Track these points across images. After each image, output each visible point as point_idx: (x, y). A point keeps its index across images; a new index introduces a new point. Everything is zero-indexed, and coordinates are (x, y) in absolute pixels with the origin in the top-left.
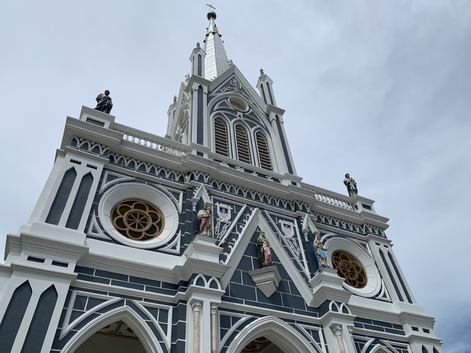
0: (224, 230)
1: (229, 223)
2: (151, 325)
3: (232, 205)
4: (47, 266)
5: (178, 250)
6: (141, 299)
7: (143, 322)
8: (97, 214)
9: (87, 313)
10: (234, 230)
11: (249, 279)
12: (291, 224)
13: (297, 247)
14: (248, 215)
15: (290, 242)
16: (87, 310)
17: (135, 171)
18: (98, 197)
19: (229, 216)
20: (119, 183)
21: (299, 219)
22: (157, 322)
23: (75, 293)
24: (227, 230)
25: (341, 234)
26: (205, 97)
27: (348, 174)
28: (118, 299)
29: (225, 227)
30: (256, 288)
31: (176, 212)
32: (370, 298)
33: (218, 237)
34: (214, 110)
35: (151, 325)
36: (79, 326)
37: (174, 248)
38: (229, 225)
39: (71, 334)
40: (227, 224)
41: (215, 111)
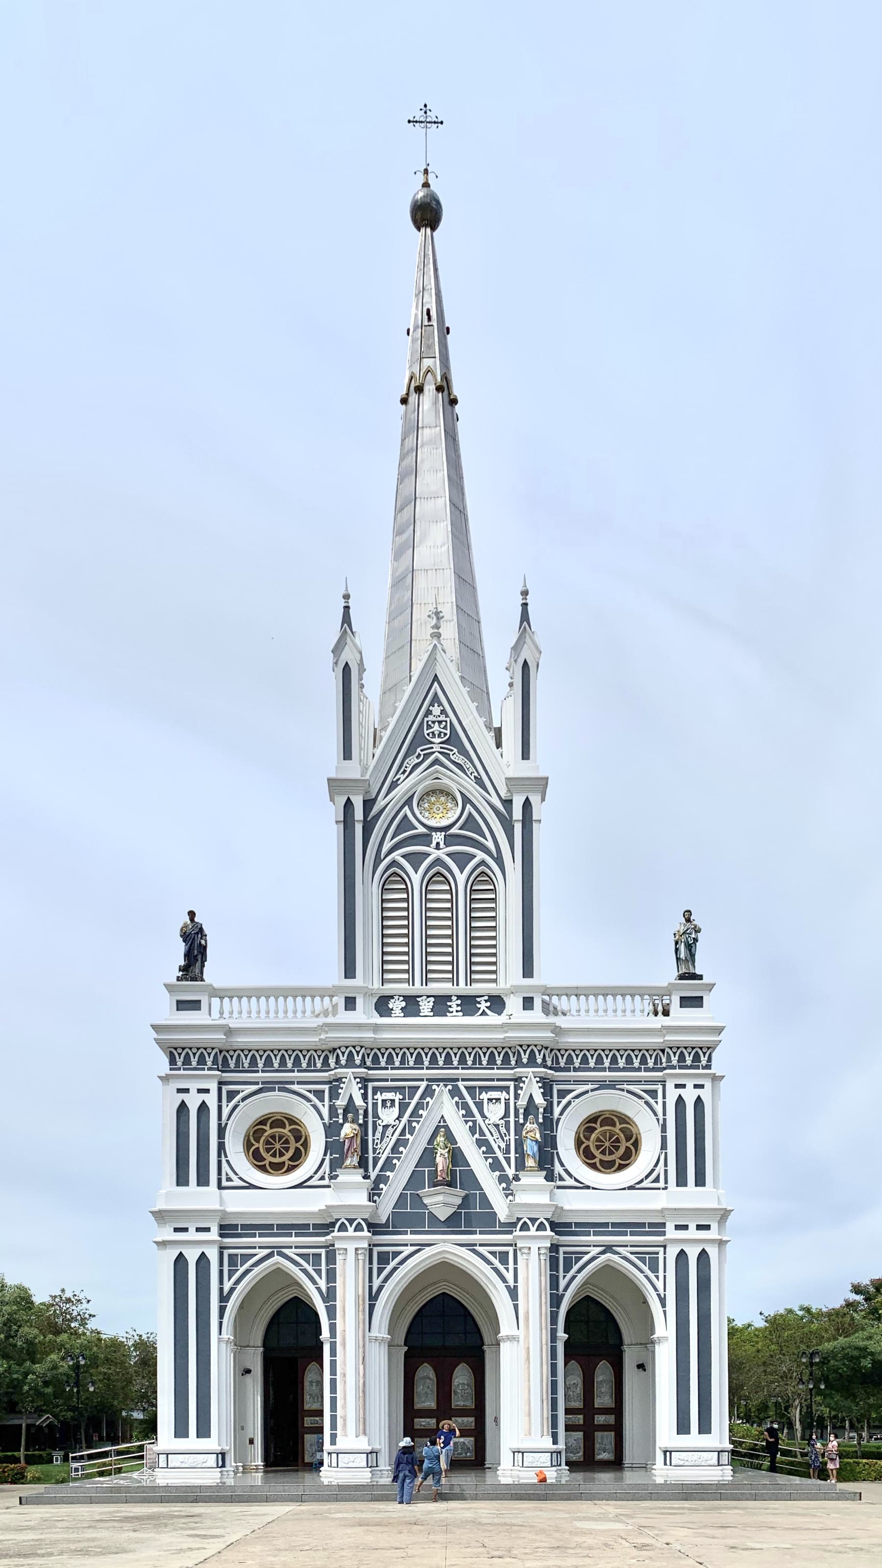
0: (388, 1137)
1: (395, 1124)
6: (291, 1247)
8: (226, 1156)
9: (242, 1270)
10: (403, 1133)
11: (418, 1200)
12: (503, 1095)
13: (505, 1134)
14: (428, 1099)
15: (493, 1129)
16: (241, 1266)
17: (257, 1071)
19: (396, 1111)
20: (243, 1099)
22: (310, 1269)
23: (226, 1253)
24: (392, 1136)
25: (609, 1081)
27: (689, 911)
28: (266, 1252)
29: (391, 1130)
30: (427, 1211)
31: (321, 1122)
32: (624, 1189)
33: (378, 1152)
34: (382, 859)
36: (237, 1282)
37: (322, 1178)
38: (395, 1128)
39: (232, 1290)
40: (393, 1127)
41: (384, 858)
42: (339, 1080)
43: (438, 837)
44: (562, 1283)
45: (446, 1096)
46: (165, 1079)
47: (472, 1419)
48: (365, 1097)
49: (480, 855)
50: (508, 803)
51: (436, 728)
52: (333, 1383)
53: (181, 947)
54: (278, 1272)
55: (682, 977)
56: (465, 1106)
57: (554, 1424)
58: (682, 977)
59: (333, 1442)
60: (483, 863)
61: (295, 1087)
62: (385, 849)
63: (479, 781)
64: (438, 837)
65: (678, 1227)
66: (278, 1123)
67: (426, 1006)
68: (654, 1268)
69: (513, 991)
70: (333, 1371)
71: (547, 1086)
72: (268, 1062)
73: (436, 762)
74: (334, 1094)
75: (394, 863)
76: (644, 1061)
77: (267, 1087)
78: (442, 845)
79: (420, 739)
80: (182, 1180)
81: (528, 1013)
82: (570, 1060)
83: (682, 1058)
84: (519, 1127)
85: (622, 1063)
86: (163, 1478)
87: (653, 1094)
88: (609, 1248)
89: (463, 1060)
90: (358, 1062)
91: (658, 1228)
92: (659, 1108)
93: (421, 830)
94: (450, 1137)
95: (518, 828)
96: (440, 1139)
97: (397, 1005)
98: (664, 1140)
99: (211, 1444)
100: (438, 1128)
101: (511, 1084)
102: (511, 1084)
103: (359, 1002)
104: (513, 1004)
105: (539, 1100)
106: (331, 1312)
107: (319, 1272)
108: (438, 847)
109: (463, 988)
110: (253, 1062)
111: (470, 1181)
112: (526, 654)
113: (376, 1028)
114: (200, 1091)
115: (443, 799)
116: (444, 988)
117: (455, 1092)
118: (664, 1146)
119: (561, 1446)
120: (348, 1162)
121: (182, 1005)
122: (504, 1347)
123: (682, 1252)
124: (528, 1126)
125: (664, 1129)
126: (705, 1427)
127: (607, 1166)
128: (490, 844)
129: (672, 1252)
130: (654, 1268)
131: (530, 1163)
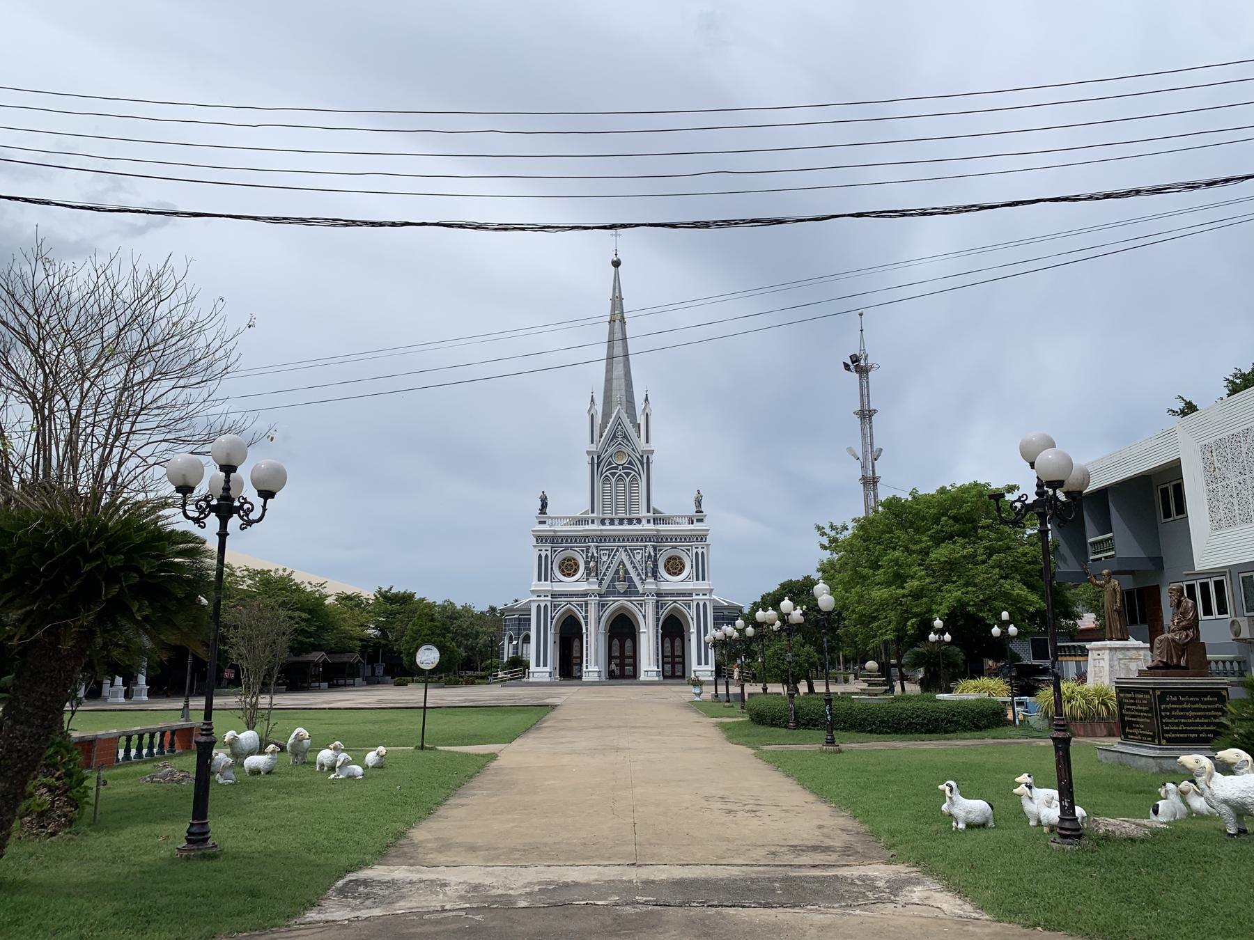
2: (578, 610)
3: (608, 550)
4: (542, 598)
5: (585, 580)
7: (575, 609)
11: (614, 586)
18: (552, 564)
20: (559, 553)
21: (646, 546)
22: (579, 609)
26: (596, 466)
35: (578, 610)
39: (555, 616)
42: (589, 547)
43: (620, 467)
44: (660, 614)
45: (623, 552)
46: (535, 546)
47: (632, 660)
48: (597, 552)
49: (634, 473)
50: (642, 456)
51: (620, 433)
52: (587, 647)
53: (540, 503)
54: (569, 610)
55: (697, 512)
56: (629, 555)
57: (658, 662)
58: (697, 512)
59: (587, 668)
60: (634, 475)
61: (575, 549)
62: (604, 470)
63: (633, 449)
64: (620, 467)
65: (696, 595)
66: (569, 560)
67: (616, 522)
68: (689, 608)
69: (644, 517)
70: (587, 644)
71: (655, 548)
72: (567, 540)
73: (620, 444)
74: (587, 551)
75: (606, 476)
76: (685, 539)
77: (567, 548)
79: (615, 437)
80: (539, 580)
81: (649, 525)
82: (662, 539)
83: (697, 539)
84: (646, 562)
85: (678, 540)
86: (531, 680)
87: (688, 550)
88: (675, 602)
89: (628, 540)
90: (595, 540)
91: (690, 595)
92: (690, 555)
93: (616, 465)
94: (624, 565)
95: (645, 465)
96: (621, 566)
97: (607, 522)
98: (692, 565)
99: (548, 669)
100: (620, 562)
101: (644, 548)
102: (644, 548)
103: (595, 522)
104: (644, 521)
105: (652, 554)
106: (586, 624)
107: (582, 610)
109: (628, 516)
110: (562, 540)
111: (631, 580)
112: (647, 410)
113: (601, 530)
114: (546, 550)
116: (622, 515)
117: (626, 550)
118: (692, 567)
119: (660, 669)
120: (592, 575)
121: (541, 523)
122: (642, 635)
123: (698, 603)
124: (649, 562)
125: (692, 562)
126: (707, 663)
127: (675, 574)
128: (637, 470)
129: (695, 603)
130: (690, 608)
131: (649, 575)
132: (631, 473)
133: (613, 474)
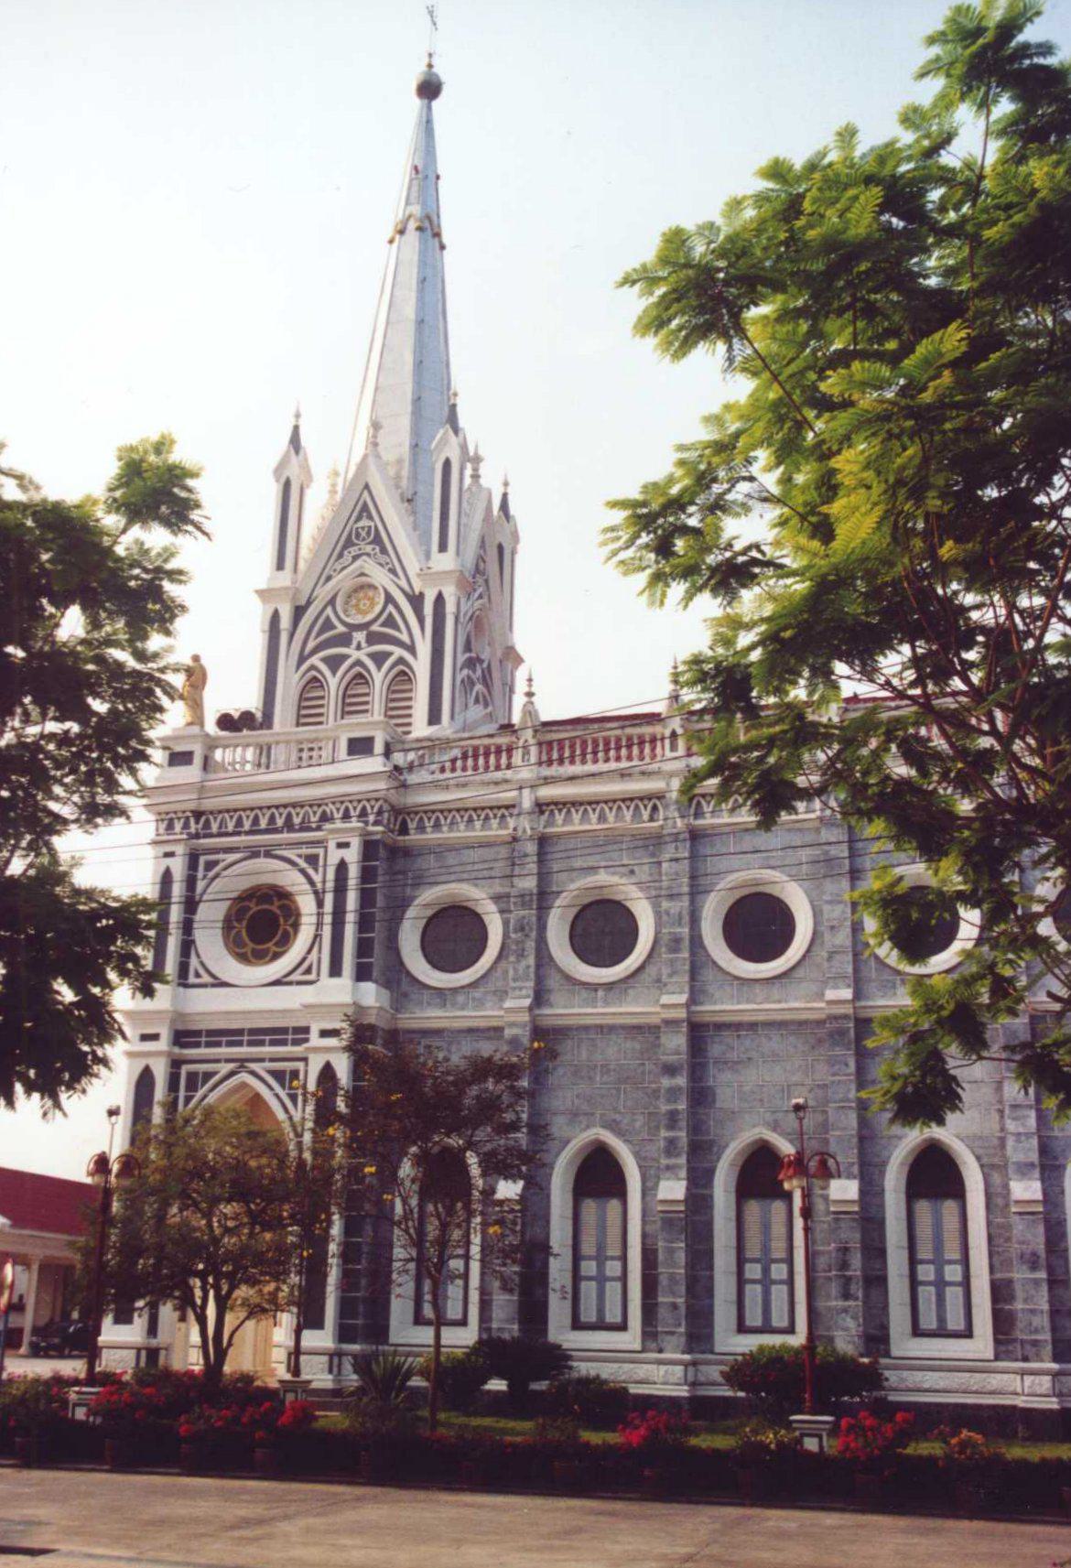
43: (360, 636)
49: (398, 652)
64: (360, 636)
78: (364, 644)
93: (341, 629)
108: (359, 647)
115: (361, 595)
128: (405, 637)
132: (389, 654)
133: (334, 663)
